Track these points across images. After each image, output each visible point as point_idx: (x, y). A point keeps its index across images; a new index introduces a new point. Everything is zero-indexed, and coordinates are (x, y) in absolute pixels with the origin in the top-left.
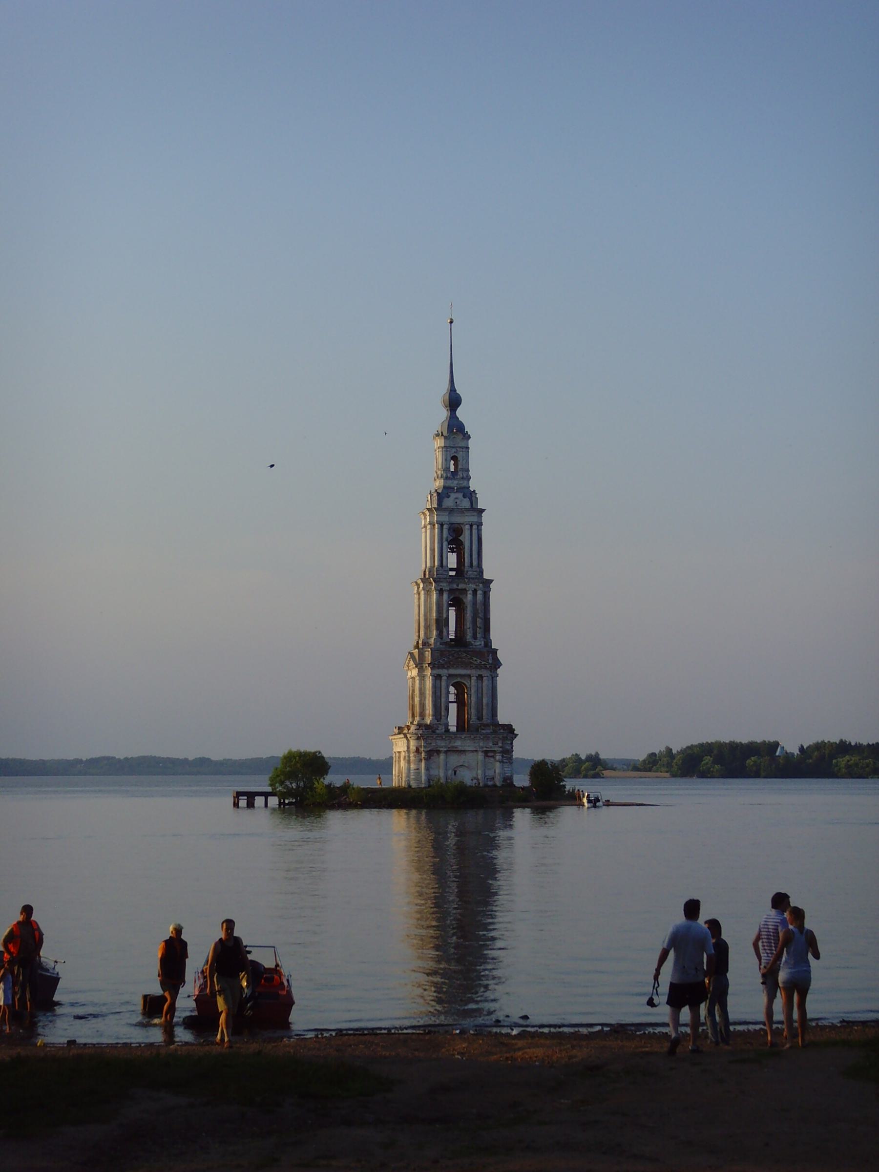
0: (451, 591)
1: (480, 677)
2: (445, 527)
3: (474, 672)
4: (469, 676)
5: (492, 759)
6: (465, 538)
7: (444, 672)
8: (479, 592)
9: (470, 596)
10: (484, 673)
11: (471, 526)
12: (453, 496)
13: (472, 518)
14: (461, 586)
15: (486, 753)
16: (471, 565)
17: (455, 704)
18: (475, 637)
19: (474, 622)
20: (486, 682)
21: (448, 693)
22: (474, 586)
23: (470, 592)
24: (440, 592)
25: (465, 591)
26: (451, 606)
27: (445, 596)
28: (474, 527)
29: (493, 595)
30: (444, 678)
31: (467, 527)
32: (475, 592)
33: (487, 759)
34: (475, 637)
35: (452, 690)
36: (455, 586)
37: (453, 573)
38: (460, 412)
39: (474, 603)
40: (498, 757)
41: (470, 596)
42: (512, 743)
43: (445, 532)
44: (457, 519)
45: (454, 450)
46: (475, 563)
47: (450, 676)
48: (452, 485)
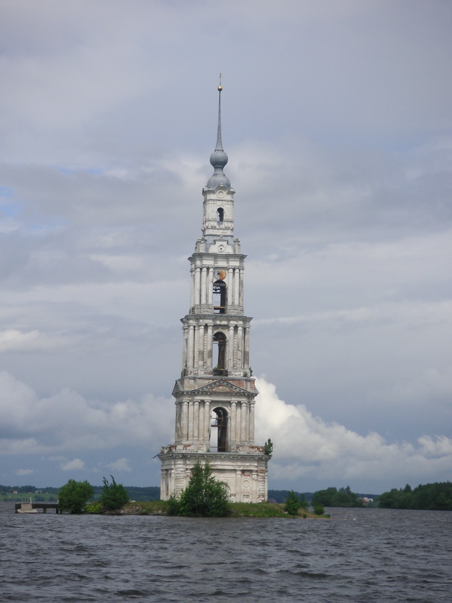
0: (215, 326)
1: (239, 404)
2: (211, 270)
3: (234, 400)
4: (230, 403)
5: (248, 477)
7: (207, 398)
10: (244, 400)
11: (234, 270)
12: (218, 243)
14: (224, 323)
16: (233, 303)
17: (217, 428)
21: (210, 417)
23: (232, 328)
24: (206, 326)
26: (215, 339)
27: (210, 331)
28: (237, 271)
30: (208, 404)
31: (231, 270)
32: (236, 327)
33: (244, 478)
35: (214, 415)
36: (218, 322)
37: (218, 311)
40: (255, 476)
41: (232, 332)
42: (266, 464)
43: (211, 274)
44: (222, 263)
45: (220, 202)
46: (236, 302)
47: (212, 402)
48: (218, 234)
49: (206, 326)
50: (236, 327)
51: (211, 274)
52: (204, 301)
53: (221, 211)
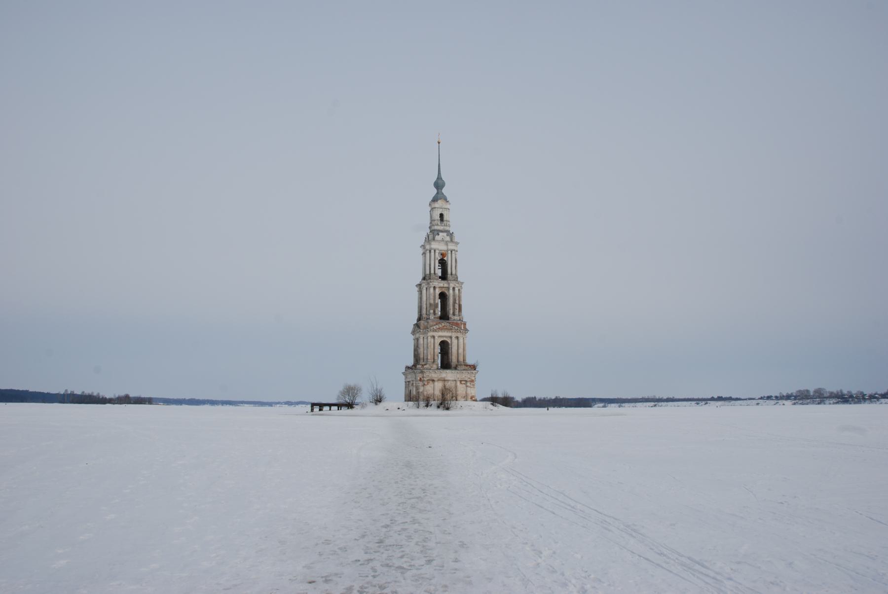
1: (457, 338)
3: (454, 335)
6: (448, 259)
7: (436, 334)
8: (457, 289)
9: (451, 291)
10: (459, 335)
13: (451, 246)
14: (446, 285)
15: (461, 381)
18: (454, 314)
19: (454, 306)
20: (461, 340)
22: (452, 285)
24: (434, 288)
25: (448, 288)
29: (463, 291)
32: (454, 288)
34: (454, 314)
36: (442, 285)
38: (444, 191)
39: (454, 295)
41: (451, 291)
44: (443, 247)
49: (434, 288)
50: (454, 288)
51: (437, 254)
52: (432, 272)
53: (441, 215)
